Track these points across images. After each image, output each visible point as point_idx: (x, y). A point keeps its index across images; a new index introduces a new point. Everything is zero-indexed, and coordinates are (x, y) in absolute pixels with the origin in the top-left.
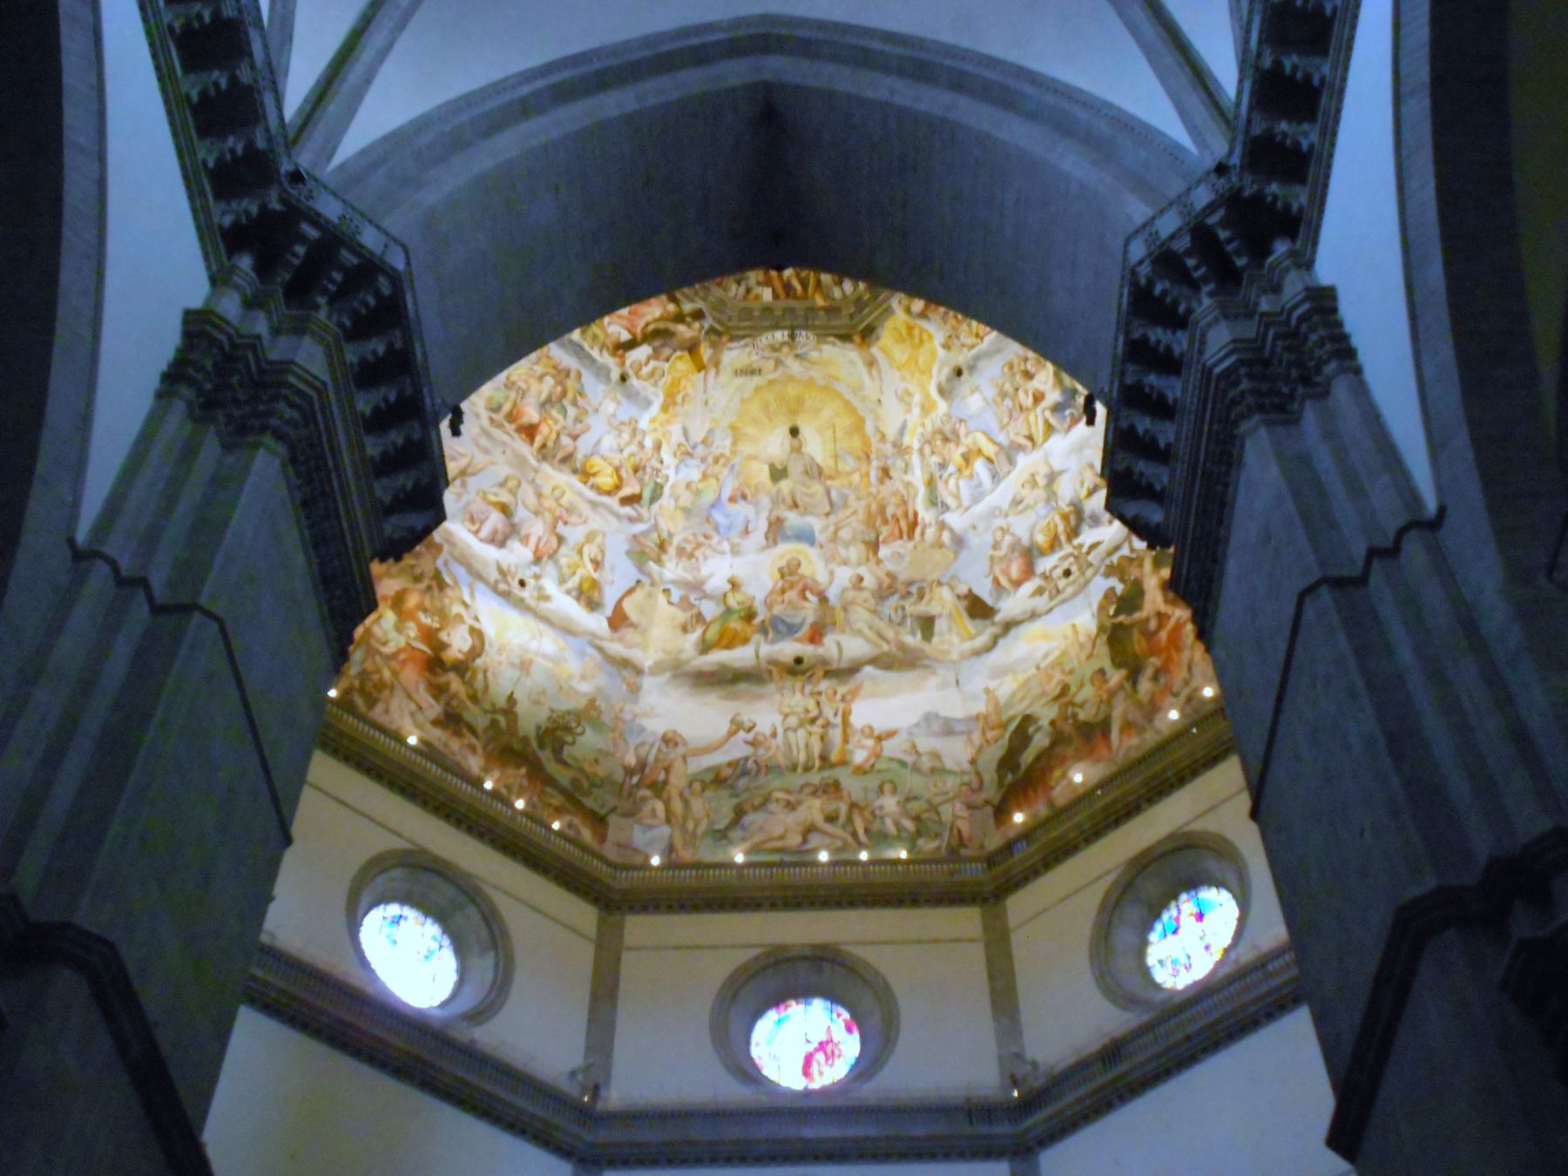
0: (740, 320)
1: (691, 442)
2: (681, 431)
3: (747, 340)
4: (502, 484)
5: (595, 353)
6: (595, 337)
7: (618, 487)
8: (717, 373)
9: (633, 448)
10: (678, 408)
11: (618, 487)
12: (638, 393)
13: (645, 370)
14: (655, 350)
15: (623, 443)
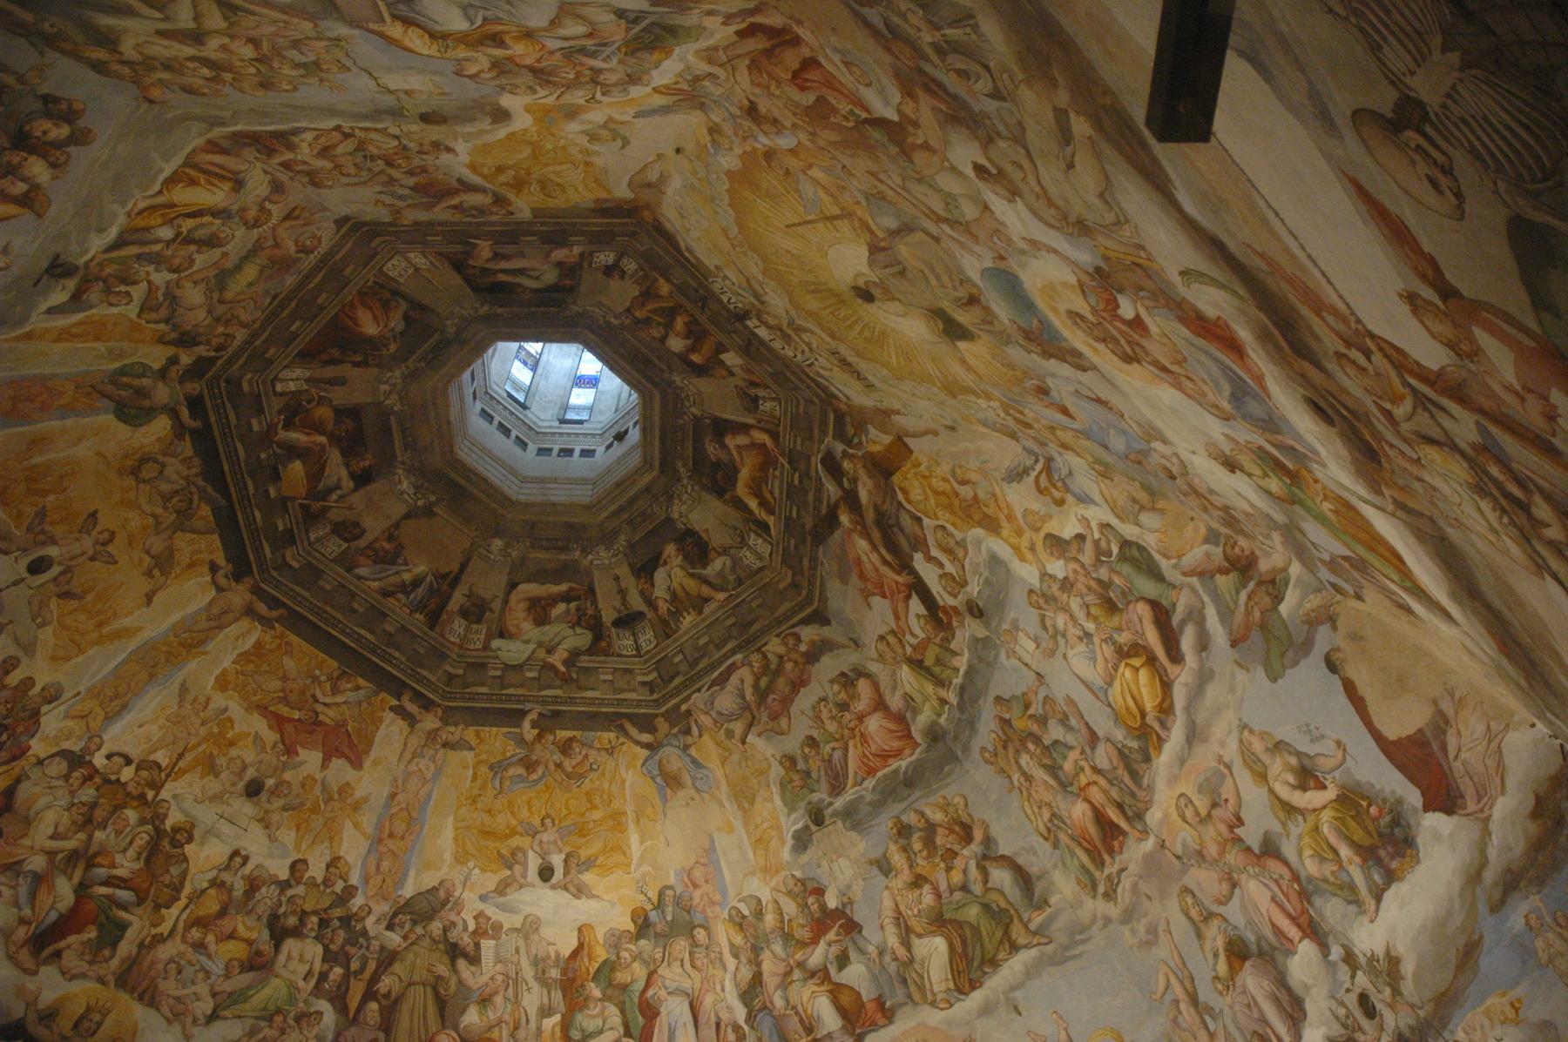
0: (796, 388)
1: (1029, 463)
2: (1014, 484)
3: (812, 375)
4: (1199, 935)
5: (962, 663)
6: (938, 661)
7: (1151, 660)
8: (897, 412)
9: (1075, 604)
10: (981, 495)
11: (1151, 660)
12: (987, 581)
13: (950, 568)
14: (915, 548)
15: (1073, 631)
